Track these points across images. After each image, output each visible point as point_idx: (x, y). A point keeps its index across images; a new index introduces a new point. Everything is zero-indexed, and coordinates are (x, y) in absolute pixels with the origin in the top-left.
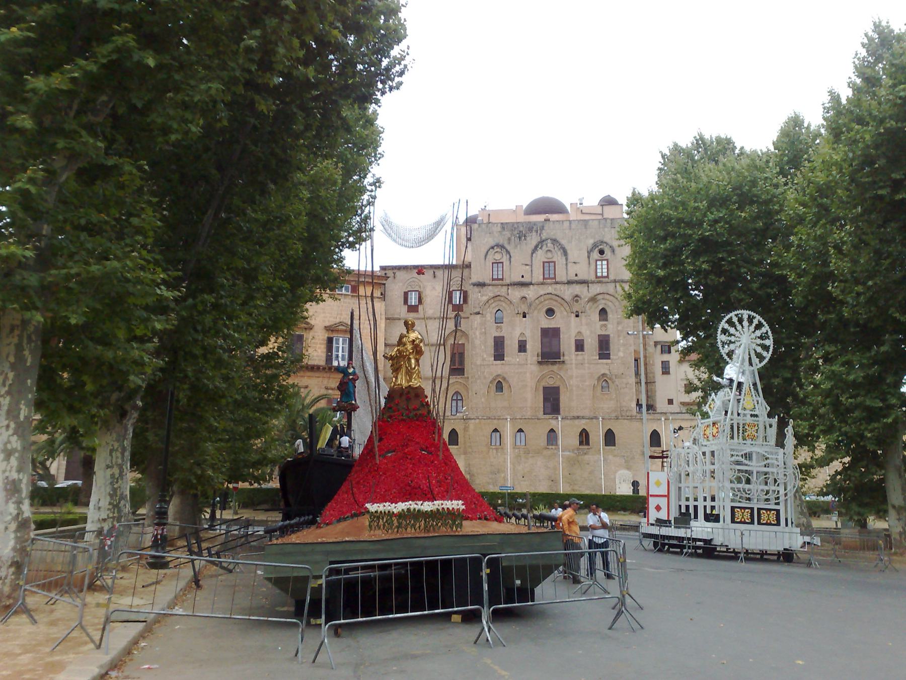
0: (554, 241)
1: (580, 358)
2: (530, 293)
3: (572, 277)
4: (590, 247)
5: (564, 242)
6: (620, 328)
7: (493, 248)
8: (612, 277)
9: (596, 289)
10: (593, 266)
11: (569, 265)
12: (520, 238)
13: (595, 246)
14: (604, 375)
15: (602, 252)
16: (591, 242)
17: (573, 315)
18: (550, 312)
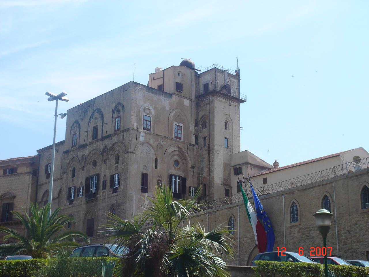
0: (99, 110)
1: (104, 194)
2: (86, 151)
3: (105, 134)
4: (113, 108)
5: (102, 110)
6: (123, 167)
7: (73, 124)
8: (122, 129)
9: (115, 139)
10: (114, 124)
11: (104, 125)
12: (85, 113)
13: (116, 108)
14: (113, 205)
15: (119, 111)
16: (114, 105)
17: (103, 163)
18: (95, 164)
